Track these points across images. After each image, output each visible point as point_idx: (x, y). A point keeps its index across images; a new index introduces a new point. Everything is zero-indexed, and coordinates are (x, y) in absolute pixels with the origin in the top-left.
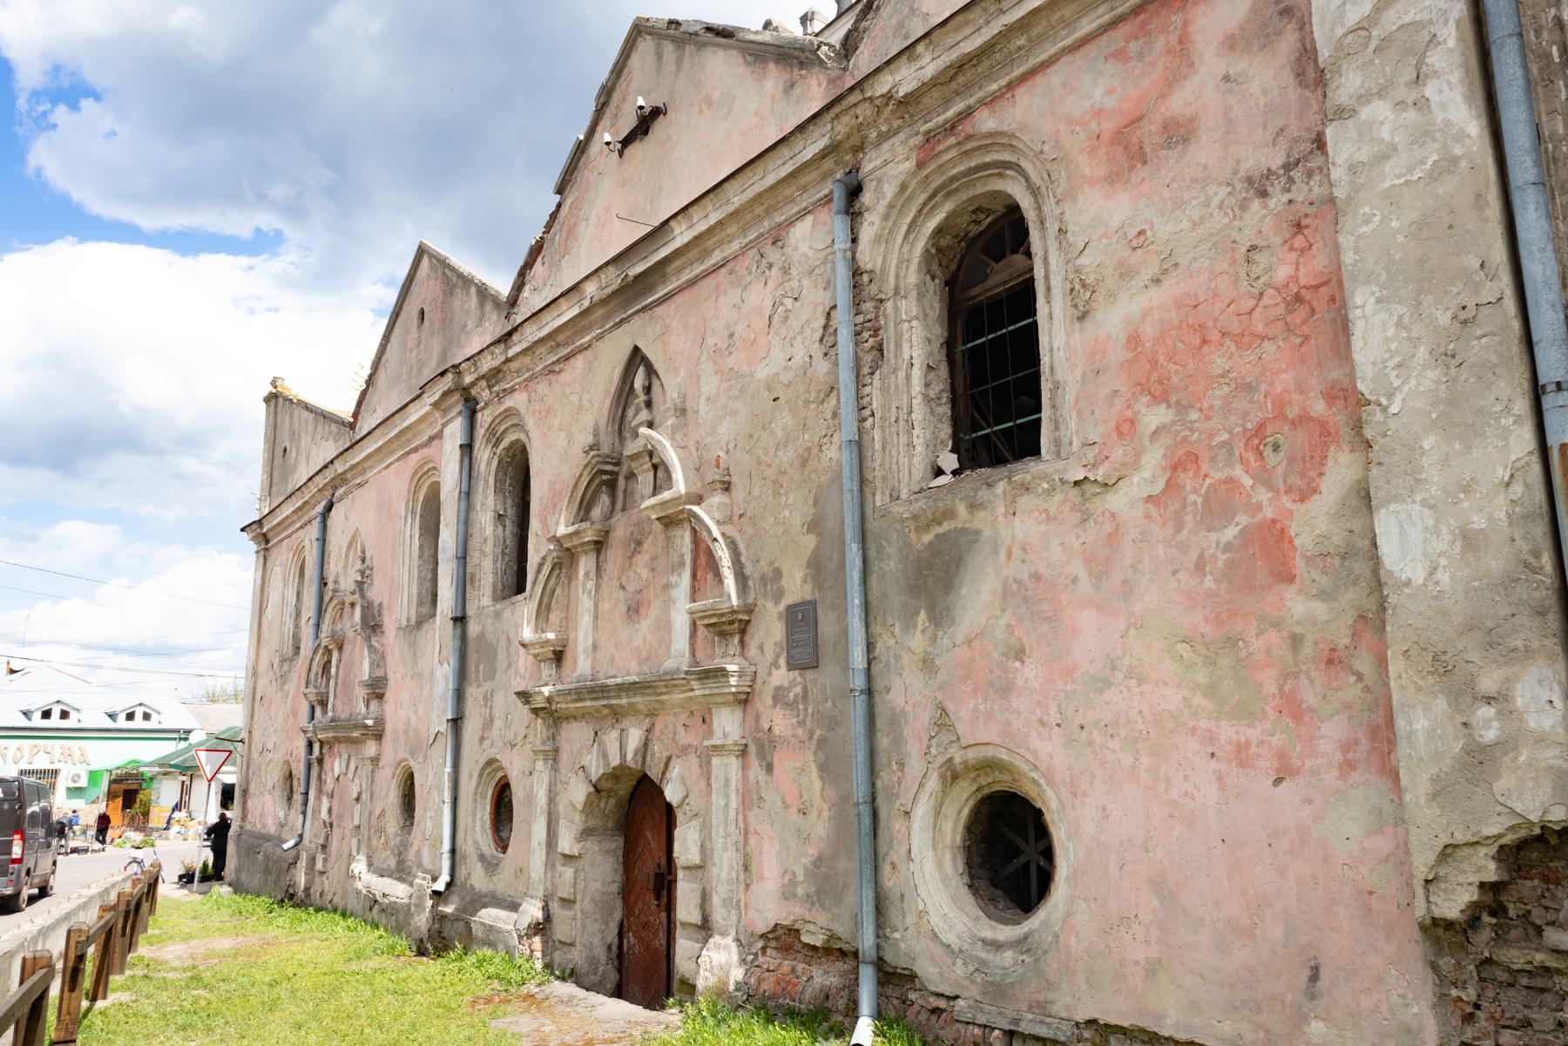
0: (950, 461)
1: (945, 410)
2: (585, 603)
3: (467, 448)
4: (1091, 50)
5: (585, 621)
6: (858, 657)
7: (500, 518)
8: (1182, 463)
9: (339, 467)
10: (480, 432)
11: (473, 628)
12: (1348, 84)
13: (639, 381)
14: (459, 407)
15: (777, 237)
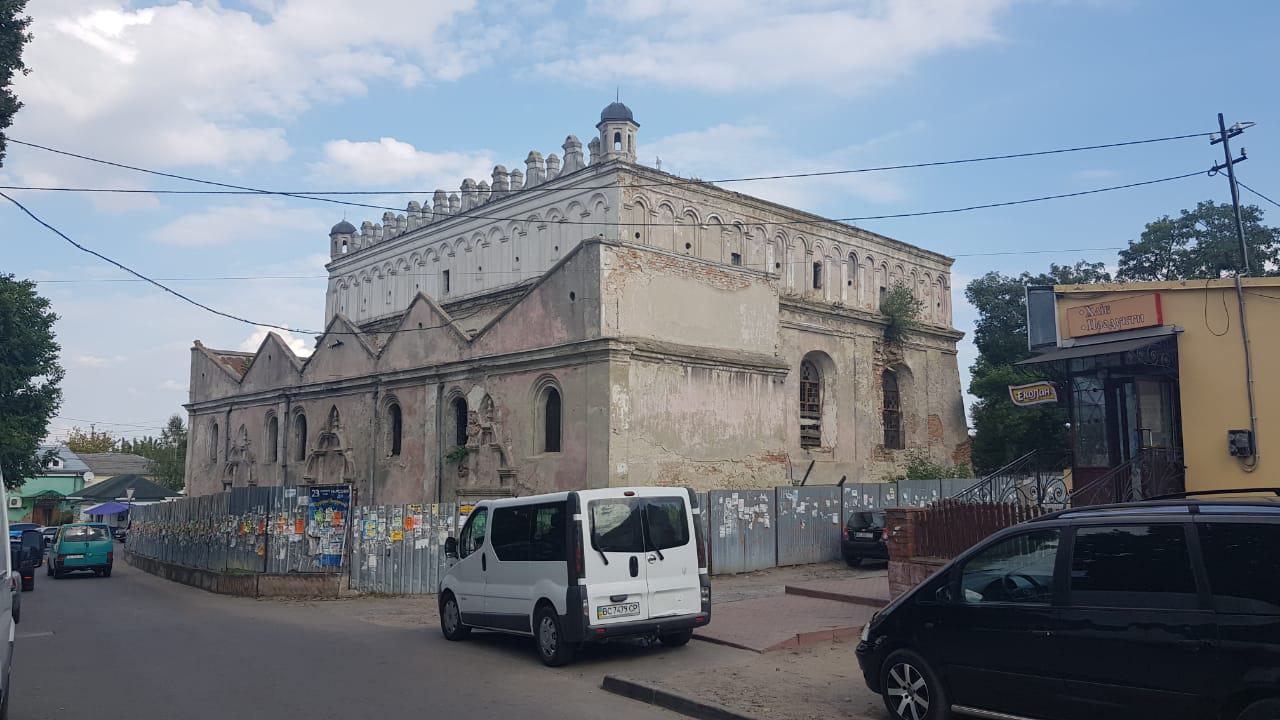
0: (391, 453)
1: (392, 442)
2: (321, 469)
3: (287, 414)
4: (407, 390)
5: (321, 474)
6: (371, 492)
7: (297, 435)
8: (411, 467)
9: (236, 400)
10: (291, 409)
11: (289, 469)
12: (427, 418)
13: (335, 413)
14: (283, 400)
15: (364, 394)
